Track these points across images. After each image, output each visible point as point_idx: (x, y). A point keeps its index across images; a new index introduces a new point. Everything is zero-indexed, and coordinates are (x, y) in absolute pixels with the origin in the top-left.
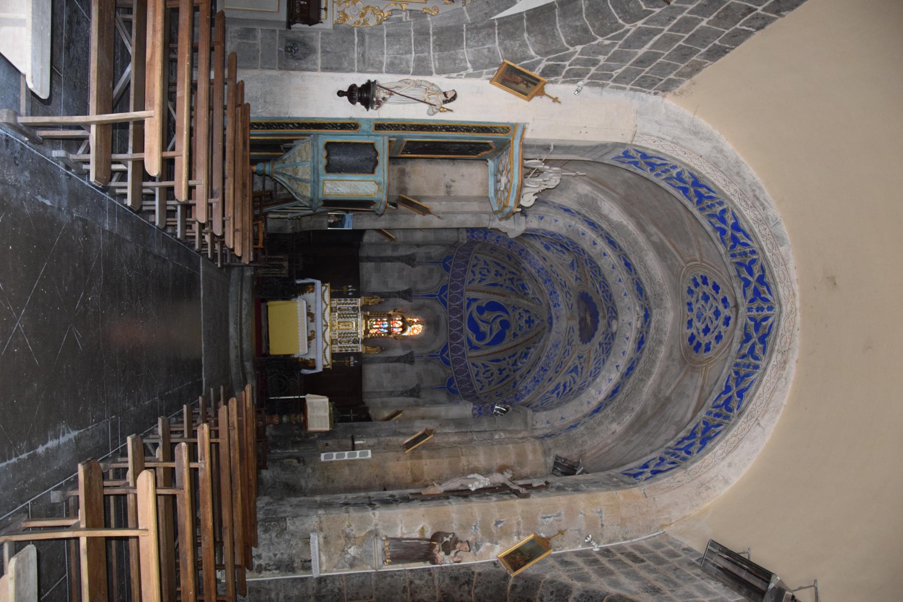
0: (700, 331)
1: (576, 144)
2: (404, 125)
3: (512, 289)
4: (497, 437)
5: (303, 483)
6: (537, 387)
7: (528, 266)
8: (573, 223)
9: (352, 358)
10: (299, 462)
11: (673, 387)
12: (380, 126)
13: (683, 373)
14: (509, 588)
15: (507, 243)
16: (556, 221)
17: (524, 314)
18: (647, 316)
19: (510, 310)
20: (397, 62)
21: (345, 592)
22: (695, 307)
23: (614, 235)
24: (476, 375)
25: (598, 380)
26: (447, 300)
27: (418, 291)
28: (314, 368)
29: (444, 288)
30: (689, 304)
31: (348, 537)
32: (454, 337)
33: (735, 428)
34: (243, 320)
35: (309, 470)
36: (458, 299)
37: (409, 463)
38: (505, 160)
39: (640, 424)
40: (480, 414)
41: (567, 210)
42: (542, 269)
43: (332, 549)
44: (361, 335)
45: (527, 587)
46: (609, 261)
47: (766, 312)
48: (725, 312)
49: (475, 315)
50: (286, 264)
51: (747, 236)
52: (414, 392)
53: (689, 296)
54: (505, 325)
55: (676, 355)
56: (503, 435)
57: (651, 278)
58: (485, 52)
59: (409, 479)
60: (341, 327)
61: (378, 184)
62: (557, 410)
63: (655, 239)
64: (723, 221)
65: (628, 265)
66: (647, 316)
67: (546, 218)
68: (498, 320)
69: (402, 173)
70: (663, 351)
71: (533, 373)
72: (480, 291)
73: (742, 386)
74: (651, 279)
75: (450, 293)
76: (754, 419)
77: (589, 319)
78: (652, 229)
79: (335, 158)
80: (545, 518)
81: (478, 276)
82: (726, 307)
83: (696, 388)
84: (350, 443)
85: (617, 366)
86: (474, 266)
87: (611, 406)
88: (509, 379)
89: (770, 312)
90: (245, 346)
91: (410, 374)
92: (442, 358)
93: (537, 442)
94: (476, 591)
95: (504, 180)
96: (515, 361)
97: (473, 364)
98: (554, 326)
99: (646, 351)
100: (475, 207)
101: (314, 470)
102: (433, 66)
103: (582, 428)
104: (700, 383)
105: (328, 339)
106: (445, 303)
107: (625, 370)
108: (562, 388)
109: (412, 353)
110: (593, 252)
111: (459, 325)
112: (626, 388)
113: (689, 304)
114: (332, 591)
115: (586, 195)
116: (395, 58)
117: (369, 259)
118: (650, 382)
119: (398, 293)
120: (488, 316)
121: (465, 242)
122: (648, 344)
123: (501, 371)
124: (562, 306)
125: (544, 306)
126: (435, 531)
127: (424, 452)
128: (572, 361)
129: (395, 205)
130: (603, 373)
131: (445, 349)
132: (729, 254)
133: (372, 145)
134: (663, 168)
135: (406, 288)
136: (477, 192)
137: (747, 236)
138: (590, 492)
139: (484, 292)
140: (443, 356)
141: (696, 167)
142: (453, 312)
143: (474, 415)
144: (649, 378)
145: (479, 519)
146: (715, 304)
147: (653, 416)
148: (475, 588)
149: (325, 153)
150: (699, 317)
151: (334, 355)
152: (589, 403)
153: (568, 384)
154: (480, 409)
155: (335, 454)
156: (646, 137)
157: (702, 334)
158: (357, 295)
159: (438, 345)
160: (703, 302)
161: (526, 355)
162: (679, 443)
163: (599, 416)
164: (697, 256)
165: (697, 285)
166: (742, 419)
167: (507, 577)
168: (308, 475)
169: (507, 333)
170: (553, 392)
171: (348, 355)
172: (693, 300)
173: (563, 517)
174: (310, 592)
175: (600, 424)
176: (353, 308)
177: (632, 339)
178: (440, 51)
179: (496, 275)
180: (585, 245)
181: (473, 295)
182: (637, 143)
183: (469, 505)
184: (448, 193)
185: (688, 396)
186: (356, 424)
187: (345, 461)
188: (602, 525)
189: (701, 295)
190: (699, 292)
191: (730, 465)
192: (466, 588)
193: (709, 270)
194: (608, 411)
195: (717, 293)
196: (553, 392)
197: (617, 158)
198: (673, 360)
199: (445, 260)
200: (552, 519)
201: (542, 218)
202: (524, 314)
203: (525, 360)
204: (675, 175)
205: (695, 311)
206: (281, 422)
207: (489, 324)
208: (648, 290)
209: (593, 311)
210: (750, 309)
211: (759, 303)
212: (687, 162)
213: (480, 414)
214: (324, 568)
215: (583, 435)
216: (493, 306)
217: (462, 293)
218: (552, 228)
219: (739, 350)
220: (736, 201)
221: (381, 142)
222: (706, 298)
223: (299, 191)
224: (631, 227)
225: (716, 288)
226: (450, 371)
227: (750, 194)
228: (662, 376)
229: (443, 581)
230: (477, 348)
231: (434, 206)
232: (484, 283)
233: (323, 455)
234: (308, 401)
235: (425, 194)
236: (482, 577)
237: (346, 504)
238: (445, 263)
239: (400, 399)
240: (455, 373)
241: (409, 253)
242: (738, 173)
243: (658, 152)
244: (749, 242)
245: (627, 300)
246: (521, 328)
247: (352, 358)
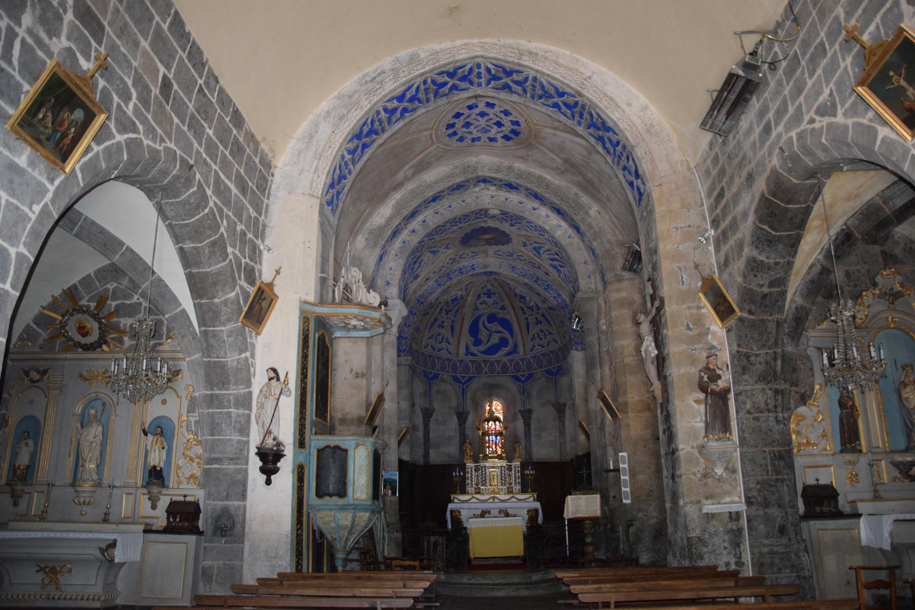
0: (500, 130)
1: (320, 252)
2: (300, 420)
3: (458, 310)
4: (604, 327)
5: (653, 521)
6: (554, 287)
7: (434, 296)
8: (393, 252)
9: (527, 472)
10: (632, 525)
11: (553, 156)
12: (301, 443)
13: (542, 148)
14: (752, 317)
15: (411, 317)
17: (482, 300)
18: (485, 180)
19: (478, 313)
20: (238, 426)
21: (760, 478)
22: (476, 134)
23: (406, 212)
24: (543, 346)
25: (547, 228)
28: (536, 510)
29: (456, 379)
30: (473, 140)
31: (705, 476)
32: (505, 369)
33: (594, 99)
34: (490, 582)
35: (640, 515)
36: (467, 366)
37: (631, 415)
38: (335, 321)
39: (590, 187)
40: (581, 343)
41: (381, 258)
42: (437, 281)
43: (718, 491)
44: (504, 463)
45: (750, 299)
46: (431, 217)
47: (483, 70)
48: (482, 106)
49: (482, 348)
50: (433, 539)
51: (409, 88)
52: (560, 409)
53: (466, 140)
54: (492, 318)
55: (521, 153)
56: (603, 321)
57: (448, 177)
58: (231, 339)
59: (647, 414)
60: (495, 483)
61: (357, 445)
62: (577, 268)
63: (409, 173)
64: (394, 110)
65: (435, 199)
66: (485, 180)
67: (388, 279)
68: (487, 324)
69: (343, 421)
70: (519, 165)
71: (541, 290)
72: (459, 343)
73: (553, 92)
74: (449, 176)
76: (585, 82)
77: (487, 236)
78: (400, 176)
79: (331, 488)
80: (683, 282)
81: (444, 345)
82: (477, 106)
84: (612, 474)
85: (534, 209)
86: (434, 349)
87: (573, 215)
88: (546, 314)
90: (516, 580)
91: (542, 413)
92: (526, 380)
93: (609, 288)
94: (755, 348)
95: (354, 322)
96: (528, 308)
97: (532, 350)
98: (494, 270)
99: (518, 181)
100: (377, 349)
101: (639, 510)
102: (243, 391)
103: (595, 243)
105: (507, 497)
106: (471, 379)
108: (555, 263)
109: (521, 412)
110: (422, 233)
111: (492, 364)
113: (473, 140)
114: (759, 491)
115: (366, 239)
116: (234, 427)
117: (426, 454)
118: (549, 177)
119: (460, 425)
120: (483, 335)
121: (410, 358)
122: (512, 180)
123: (538, 322)
124: (474, 262)
125: (473, 280)
126: (698, 390)
127: (620, 400)
128: (528, 252)
129: (374, 429)
130: (540, 223)
131: (517, 378)
132: (426, 105)
133: (319, 451)
134: (344, 168)
135: (455, 417)
136: (362, 347)
137: (409, 88)
138: (657, 239)
139: (459, 339)
140: (523, 380)
141: (343, 137)
142: (479, 370)
143: (582, 349)
144: (545, 179)
145: (685, 346)
146: (474, 116)
147: (581, 174)
148: (752, 349)
149: (327, 498)
150: (486, 131)
151: (524, 491)
152: (570, 237)
153: (551, 257)
154: (577, 343)
155: (623, 489)
156: (314, 185)
157: (503, 129)
158: (463, 467)
159: (512, 386)
160: (472, 127)
161: (522, 297)
162: (608, 152)
163: (583, 227)
164: (427, 133)
165: (455, 133)
166: (585, 93)
167: (741, 319)
168: (645, 516)
169: (501, 316)
170: (559, 271)
171: (523, 477)
172: (469, 136)
173: (682, 265)
174: (761, 513)
175: (590, 226)
176: (476, 470)
177: (507, 195)
178: (229, 383)
179: (443, 327)
180: (415, 240)
181: (462, 350)
182: (320, 193)
183: (671, 356)
184: (363, 375)
185: (563, 142)
186: (593, 468)
187: (630, 479)
188: (689, 226)
189: (464, 129)
190: (461, 131)
191: (629, 105)
192: (753, 359)
193: (441, 121)
194: (578, 218)
195: (463, 114)
196: (559, 271)
197: (333, 211)
198: (528, 155)
199: (428, 378)
200: (684, 276)
201: (388, 283)
202: (482, 300)
203: (528, 299)
204: (350, 157)
205: (479, 135)
206: (592, 544)
207: (492, 334)
208: (459, 180)
209: (480, 232)
210: (479, 85)
211: (473, 77)
212: (338, 145)
213: (581, 343)
214: (737, 499)
216: (474, 330)
217: (461, 361)
218: (398, 273)
219: (518, 94)
220: (376, 99)
221: (316, 442)
222: (468, 125)
223: (363, 524)
224: (397, 196)
225: (458, 115)
227: (370, 86)
228: (543, 166)
229: (746, 381)
230: (516, 346)
231: (376, 389)
232: (451, 340)
233: (625, 501)
234: (571, 516)
235: (364, 399)
236: (742, 343)
237: (673, 477)
238: (431, 378)
239: (567, 423)
241: (420, 414)
242: (350, 97)
243: (328, 173)
244: (415, 86)
245: (468, 200)
246: (495, 303)
247: (527, 472)
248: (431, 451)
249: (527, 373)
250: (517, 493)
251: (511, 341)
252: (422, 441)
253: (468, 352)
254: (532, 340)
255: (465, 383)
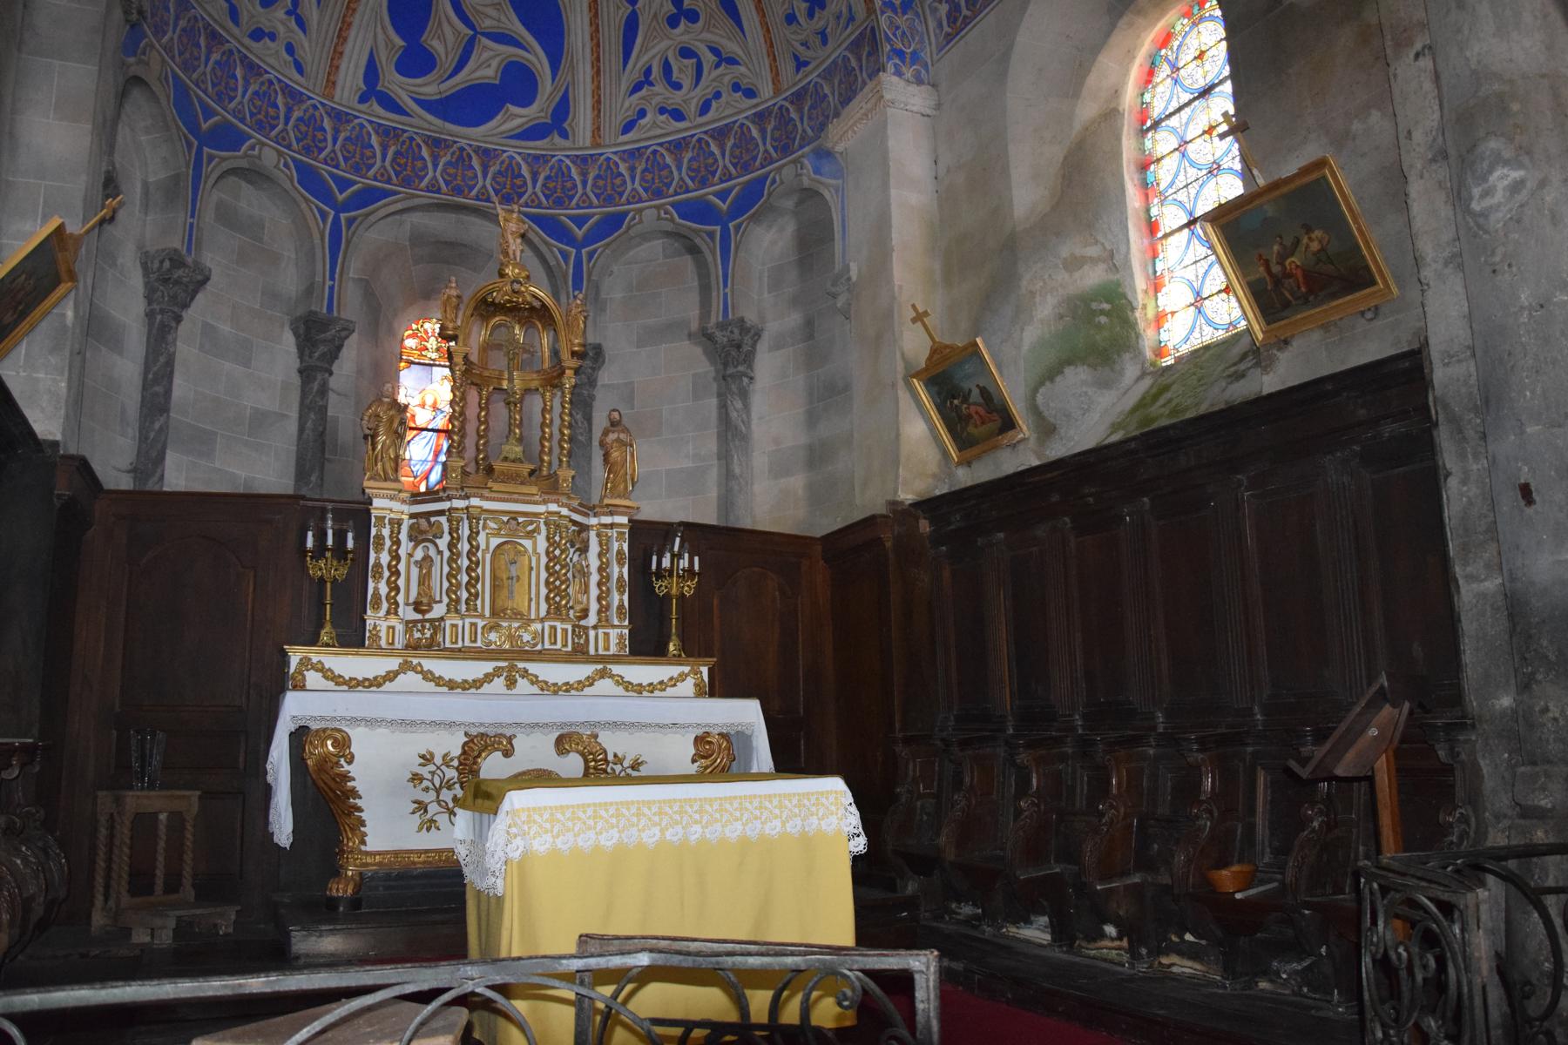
24: (678, 115)
26: (361, 183)
27: (309, 291)
29: (309, 178)
49: (430, 87)
72: (342, 37)
75: (332, 161)
92: (591, 239)
97: (628, 127)
106: (369, 197)
111: (462, 159)
117: (150, 458)
119: (306, 373)
135: (289, 340)
139: (345, 25)
142: (407, 169)
151: (646, 646)
154: (900, 54)
176: (417, 536)
199: (194, 128)
217: (339, 117)
226: (650, 215)
230: (562, 110)
238: (209, 139)
240: (658, 194)
241: (137, 281)
248: (171, 458)
249: (598, 212)
250: (617, 659)
251: (546, 86)
252: (131, 397)
253: (371, 89)
254: (637, 88)
255: (346, 207)
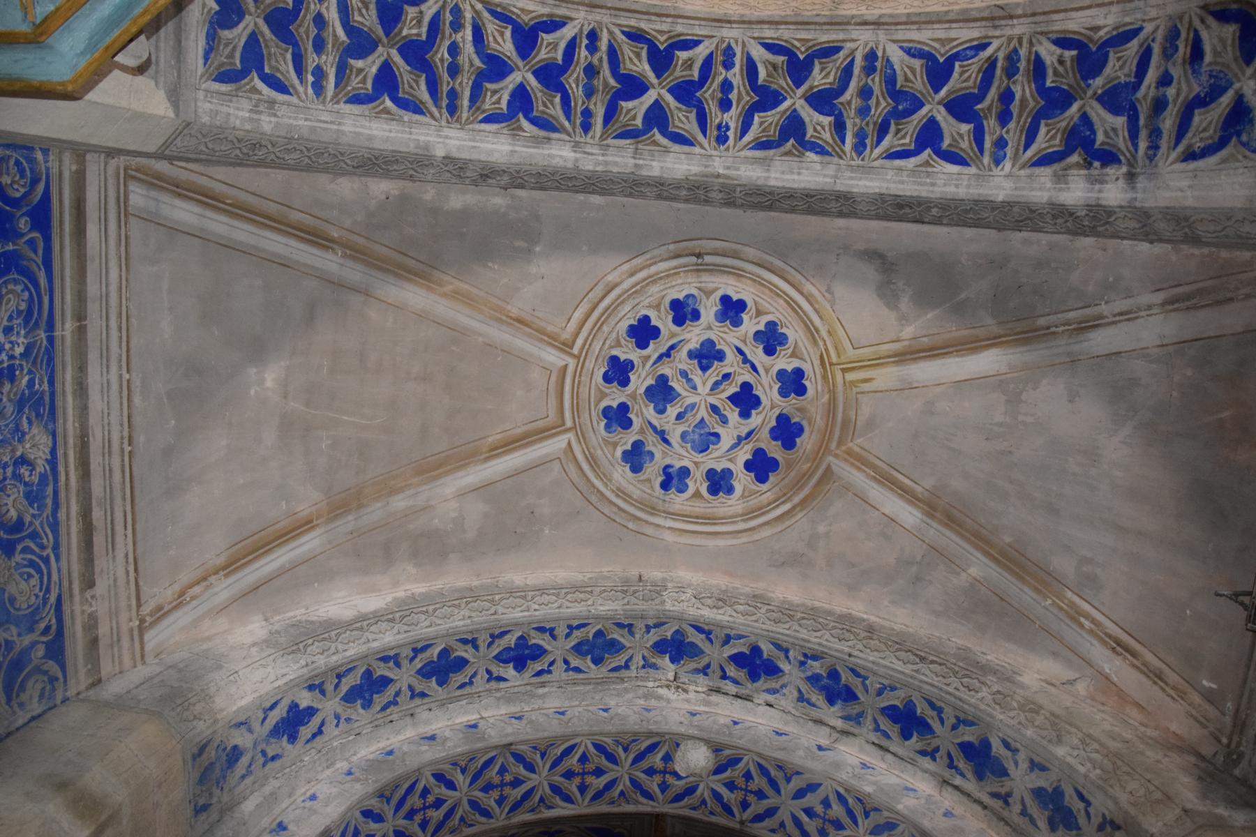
8: (342, 765)
13: (858, 478)
16: (313, 798)
22: (682, 456)
47: (736, 76)
57: (576, 588)
65: (522, 655)
83: (907, 388)
85: (820, 748)
89: (737, 60)
104: (886, 377)
107: (833, 715)
110: (456, 746)
112: (899, 666)
146: (682, 360)
164: (554, 358)
189: (650, 412)
215: (1087, 739)
219: (822, 151)
